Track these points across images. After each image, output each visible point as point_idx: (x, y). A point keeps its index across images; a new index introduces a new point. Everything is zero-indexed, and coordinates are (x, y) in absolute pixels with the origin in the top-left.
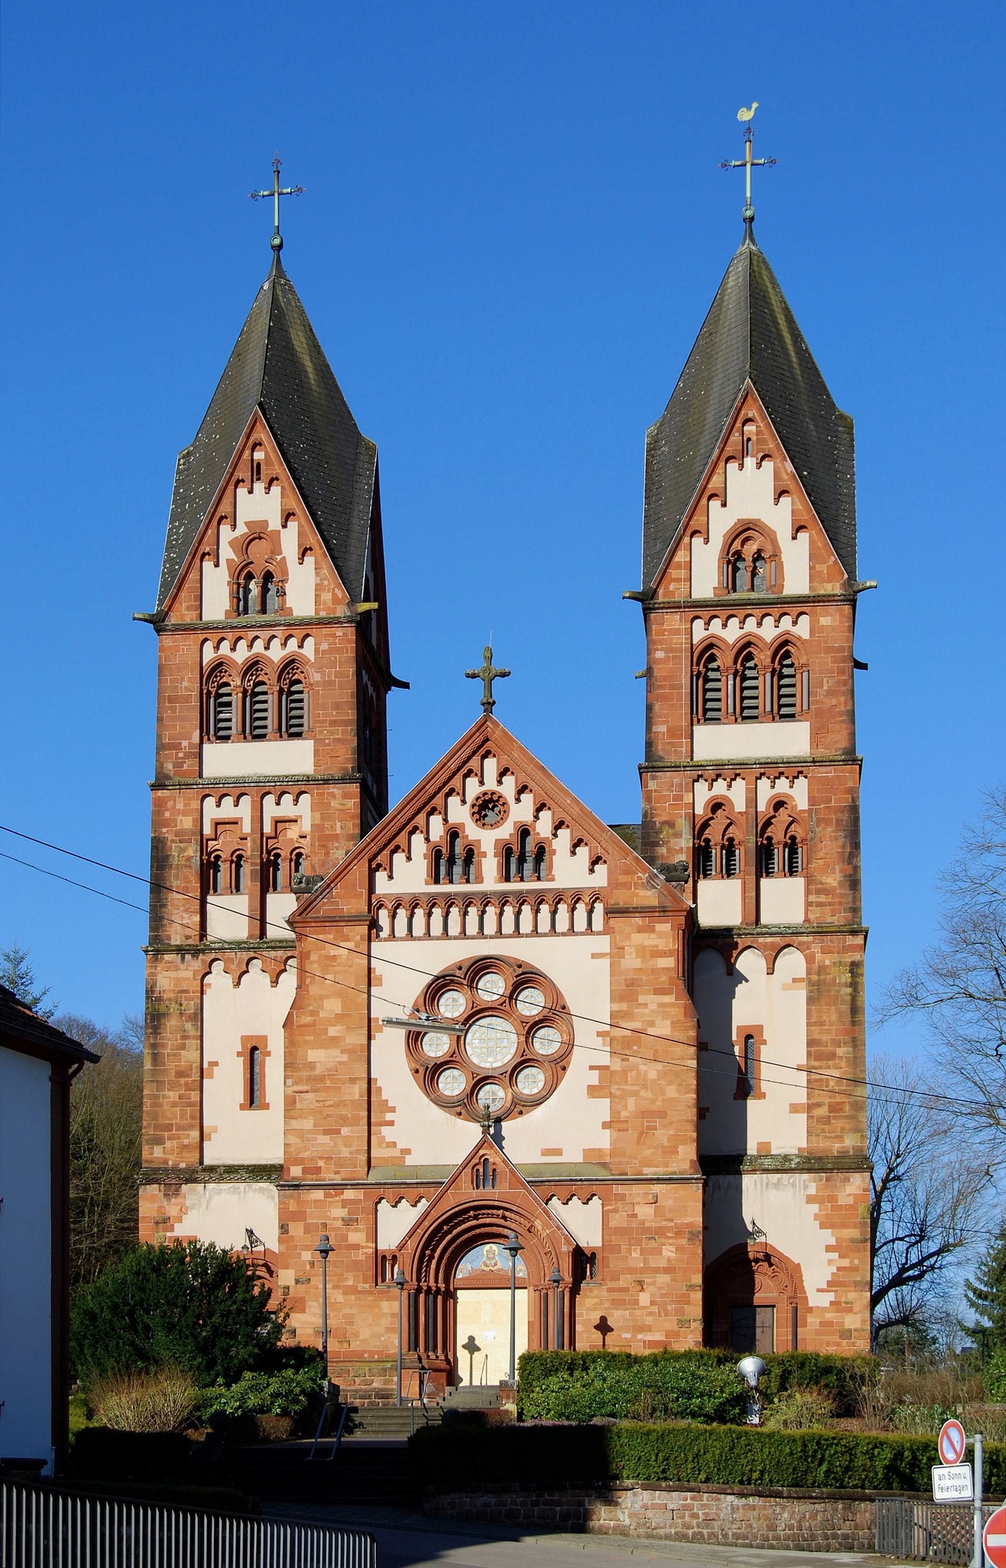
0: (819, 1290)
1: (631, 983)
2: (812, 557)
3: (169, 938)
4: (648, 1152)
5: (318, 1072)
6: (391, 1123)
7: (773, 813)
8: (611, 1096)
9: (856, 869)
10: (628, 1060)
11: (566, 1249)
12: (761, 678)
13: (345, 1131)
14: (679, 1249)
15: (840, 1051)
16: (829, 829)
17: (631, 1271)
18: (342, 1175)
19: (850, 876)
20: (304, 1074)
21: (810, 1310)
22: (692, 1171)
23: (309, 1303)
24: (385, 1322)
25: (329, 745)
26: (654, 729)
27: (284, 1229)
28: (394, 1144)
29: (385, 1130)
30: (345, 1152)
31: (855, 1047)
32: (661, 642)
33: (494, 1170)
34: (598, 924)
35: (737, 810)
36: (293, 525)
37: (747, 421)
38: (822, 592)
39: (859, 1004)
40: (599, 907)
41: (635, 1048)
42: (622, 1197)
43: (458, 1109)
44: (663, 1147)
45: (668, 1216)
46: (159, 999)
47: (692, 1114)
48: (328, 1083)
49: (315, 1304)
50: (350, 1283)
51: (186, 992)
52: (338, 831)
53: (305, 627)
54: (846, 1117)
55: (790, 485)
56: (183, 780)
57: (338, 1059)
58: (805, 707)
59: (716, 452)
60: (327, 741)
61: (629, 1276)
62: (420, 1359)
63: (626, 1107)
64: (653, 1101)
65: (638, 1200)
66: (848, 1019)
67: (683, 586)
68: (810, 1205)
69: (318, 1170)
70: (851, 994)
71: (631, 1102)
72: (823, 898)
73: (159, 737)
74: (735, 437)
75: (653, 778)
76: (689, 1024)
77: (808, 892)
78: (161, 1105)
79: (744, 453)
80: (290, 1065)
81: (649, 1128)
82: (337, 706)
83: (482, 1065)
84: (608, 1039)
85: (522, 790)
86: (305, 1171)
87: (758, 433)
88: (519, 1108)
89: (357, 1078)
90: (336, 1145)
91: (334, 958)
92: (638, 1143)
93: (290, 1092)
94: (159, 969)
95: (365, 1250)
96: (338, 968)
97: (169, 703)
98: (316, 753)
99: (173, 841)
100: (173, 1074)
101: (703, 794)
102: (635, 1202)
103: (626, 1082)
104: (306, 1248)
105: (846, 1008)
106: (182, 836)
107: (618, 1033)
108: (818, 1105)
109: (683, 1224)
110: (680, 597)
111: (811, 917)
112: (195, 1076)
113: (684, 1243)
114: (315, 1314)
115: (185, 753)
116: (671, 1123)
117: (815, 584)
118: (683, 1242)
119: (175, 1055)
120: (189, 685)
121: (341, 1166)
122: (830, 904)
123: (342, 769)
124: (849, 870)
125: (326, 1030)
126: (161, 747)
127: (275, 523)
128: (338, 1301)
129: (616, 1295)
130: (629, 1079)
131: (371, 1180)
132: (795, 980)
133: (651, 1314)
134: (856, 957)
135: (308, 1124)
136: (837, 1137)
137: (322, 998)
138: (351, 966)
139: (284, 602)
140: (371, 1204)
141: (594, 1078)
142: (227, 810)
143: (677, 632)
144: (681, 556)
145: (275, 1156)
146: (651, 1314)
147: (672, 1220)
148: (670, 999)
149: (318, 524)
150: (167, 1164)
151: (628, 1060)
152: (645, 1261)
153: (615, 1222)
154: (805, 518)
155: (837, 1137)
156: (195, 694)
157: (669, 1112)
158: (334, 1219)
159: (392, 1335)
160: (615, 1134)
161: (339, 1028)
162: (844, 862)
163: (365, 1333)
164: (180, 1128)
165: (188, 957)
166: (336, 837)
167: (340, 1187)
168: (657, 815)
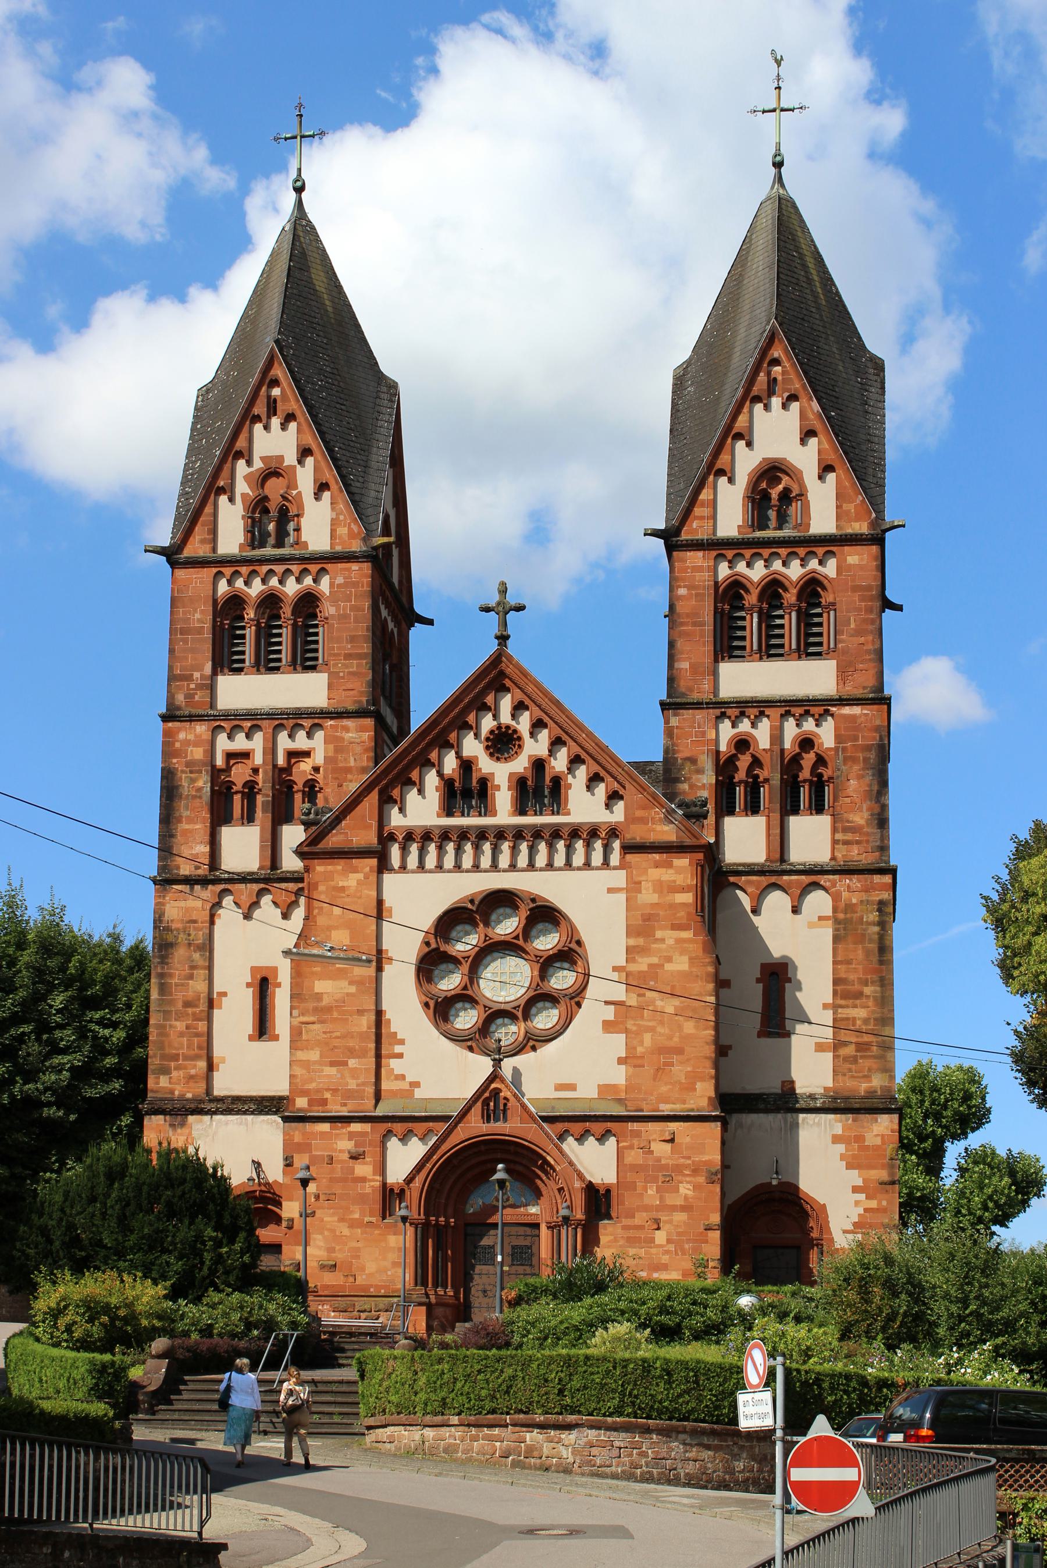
2: (839, 496)
4: (664, 1089)
6: (400, 1056)
8: (626, 1031)
9: (884, 808)
10: (644, 995)
11: (578, 1184)
12: (787, 617)
13: (352, 1063)
14: (696, 1187)
15: (868, 990)
16: (856, 768)
17: (646, 1208)
18: (350, 1107)
19: (879, 814)
20: (311, 1005)
22: (711, 1108)
25: (343, 678)
26: (676, 665)
27: (288, 1163)
28: (403, 1077)
29: (394, 1063)
30: (352, 1084)
32: (683, 579)
33: (505, 1105)
34: (615, 859)
35: (761, 747)
36: (310, 461)
37: (776, 362)
38: (850, 531)
39: (888, 943)
40: (616, 845)
42: (637, 1134)
44: (681, 1083)
45: (685, 1153)
47: (709, 1051)
48: (335, 1015)
49: (320, 1237)
50: (357, 1216)
52: (352, 763)
55: (818, 426)
56: (194, 711)
57: (346, 991)
58: (832, 645)
60: (341, 674)
61: (644, 1214)
62: (427, 1295)
63: (642, 1043)
64: (670, 1038)
65: (654, 1136)
66: (875, 958)
67: (708, 525)
69: (324, 1102)
71: (647, 1038)
72: (849, 837)
73: (171, 668)
74: (762, 377)
75: (675, 715)
76: (707, 960)
77: (834, 830)
79: (771, 393)
80: (296, 996)
81: (666, 1064)
82: (353, 639)
83: (495, 999)
85: (538, 725)
86: (311, 1102)
87: (784, 373)
88: (531, 1043)
92: (654, 1080)
93: (296, 1022)
95: (372, 1184)
97: (181, 634)
98: (330, 686)
99: (183, 772)
101: (726, 732)
103: (642, 1017)
105: (874, 946)
107: (633, 968)
108: (845, 1044)
110: (702, 535)
111: (838, 855)
112: (203, 1006)
114: (319, 1248)
115: (197, 685)
116: (688, 1060)
117: (843, 523)
118: (701, 1179)
120: (201, 617)
121: (348, 1098)
122: (858, 842)
123: (355, 702)
124: (877, 810)
126: (172, 678)
129: (631, 1233)
131: (379, 1112)
132: (820, 918)
133: (667, 1252)
135: (314, 1055)
137: (330, 928)
139: (299, 537)
140: (378, 1137)
141: (609, 1013)
143: (700, 569)
144: (705, 495)
145: (279, 1087)
146: (667, 1252)
147: (689, 1158)
149: (334, 460)
151: (644, 995)
152: (661, 1199)
153: (630, 1159)
154: (831, 458)
156: (208, 625)
157: (686, 1048)
158: (341, 1151)
160: (631, 1070)
162: (871, 800)
163: (371, 1267)
166: (348, 770)
168: (678, 751)
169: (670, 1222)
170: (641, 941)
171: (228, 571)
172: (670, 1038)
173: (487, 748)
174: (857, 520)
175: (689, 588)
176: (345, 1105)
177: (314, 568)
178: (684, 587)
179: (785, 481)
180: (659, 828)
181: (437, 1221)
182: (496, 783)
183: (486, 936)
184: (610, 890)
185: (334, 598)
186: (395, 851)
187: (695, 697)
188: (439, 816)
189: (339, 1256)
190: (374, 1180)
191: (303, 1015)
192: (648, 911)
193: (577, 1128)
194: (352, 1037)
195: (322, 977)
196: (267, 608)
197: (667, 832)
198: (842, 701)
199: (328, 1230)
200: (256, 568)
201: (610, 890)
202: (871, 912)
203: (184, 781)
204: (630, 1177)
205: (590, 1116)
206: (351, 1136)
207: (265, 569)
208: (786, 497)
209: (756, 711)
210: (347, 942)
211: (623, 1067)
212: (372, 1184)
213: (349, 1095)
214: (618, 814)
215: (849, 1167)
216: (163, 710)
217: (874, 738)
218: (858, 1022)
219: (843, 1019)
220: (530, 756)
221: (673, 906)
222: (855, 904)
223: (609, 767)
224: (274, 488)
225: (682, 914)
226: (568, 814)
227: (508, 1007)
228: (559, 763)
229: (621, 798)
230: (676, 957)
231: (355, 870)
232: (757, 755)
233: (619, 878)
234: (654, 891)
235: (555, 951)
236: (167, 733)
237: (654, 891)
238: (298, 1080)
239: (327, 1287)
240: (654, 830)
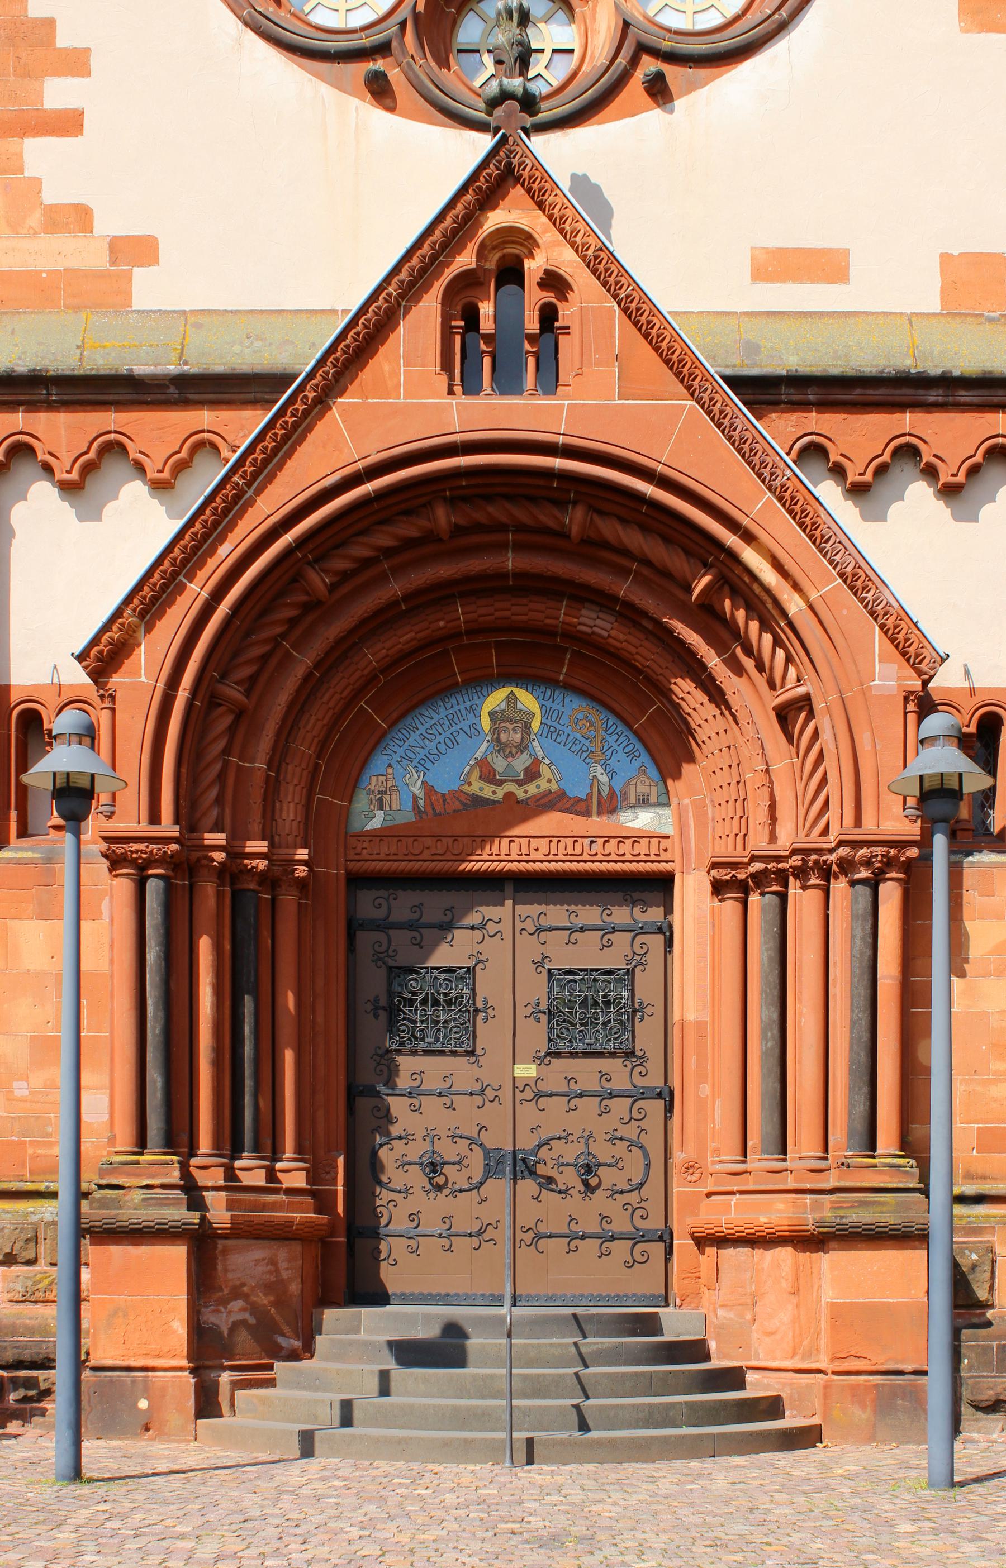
33: (548, 316)
88: (649, 65)
181: (235, 853)
205: (922, 382)
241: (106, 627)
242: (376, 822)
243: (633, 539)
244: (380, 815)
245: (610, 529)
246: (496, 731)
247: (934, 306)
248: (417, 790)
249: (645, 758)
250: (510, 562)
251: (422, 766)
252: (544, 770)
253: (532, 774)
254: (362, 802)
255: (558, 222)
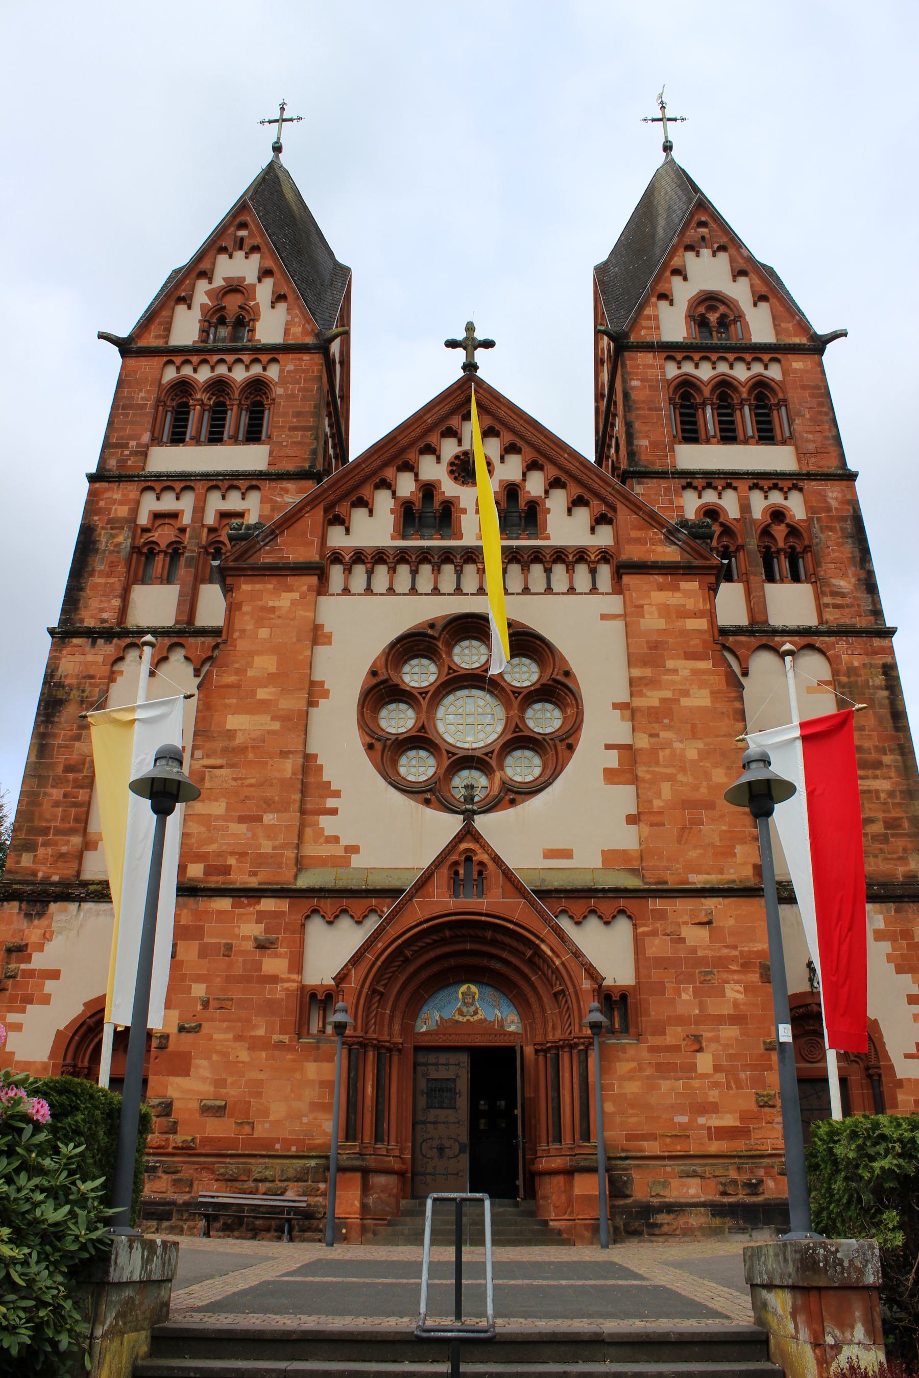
0: (908, 1056)
1: (655, 646)
3: (82, 621)
4: (693, 854)
5: (240, 740)
6: (334, 812)
7: (770, 521)
9: (870, 574)
10: (657, 735)
13: (268, 818)
15: (887, 759)
17: (681, 1020)
19: (866, 580)
20: (219, 745)
21: (900, 1083)
23: (196, 1062)
24: (311, 1094)
25: (286, 446)
26: (635, 442)
28: (336, 840)
29: (325, 821)
30: (267, 847)
31: (903, 754)
32: (636, 374)
33: (480, 873)
39: (900, 708)
41: (666, 721)
42: (661, 915)
43: (428, 796)
45: (729, 941)
46: (60, 685)
48: (251, 756)
49: (204, 1063)
50: (261, 1032)
51: (92, 677)
53: (274, 352)
54: (908, 835)
57: (267, 728)
58: (787, 434)
59: (675, 240)
60: (285, 444)
61: (679, 1029)
63: (659, 795)
65: (686, 918)
66: (889, 724)
68: (879, 943)
69: (226, 870)
70: (888, 698)
71: (666, 789)
73: (107, 438)
75: (639, 483)
76: (733, 695)
77: (817, 597)
78: (39, 805)
82: (298, 415)
84: (627, 713)
89: (290, 752)
90: (255, 837)
91: (273, 609)
92: (679, 841)
94: (64, 652)
95: (286, 985)
96: (278, 621)
97: (123, 409)
99: (103, 528)
100: (59, 770)
102: (680, 921)
103: (657, 763)
104: (199, 979)
105: (885, 712)
106: (115, 524)
107: (638, 702)
109: (750, 952)
113: (755, 980)
114: (204, 1079)
116: (722, 816)
118: (755, 977)
119: (66, 747)
123: (297, 467)
124: (863, 575)
125: (253, 693)
127: (251, 277)
128: (241, 1059)
129: (663, 1058)
130: (661, 759)
131: (303, 882)
133: (716, 1085)
134: (889, 660)
136: (900, 858)
137: (252, 654)
138: (294, 619)
142: (168, 503)
143: (652, 367)
144: (648, 311)
146: (716, 1085)
147: (735, 947)
148: (706, 665)
150: (35, 875)
151: (657, 735)
152: (702, 1006)
155: (900, 858)
158: (245, 938)
159: (321, 1115)
160: (646, 830)
161: (271, 689)
163: (278, 1110)
164: (58, 832)
165: (100, 642)
167: (255, 894)
169: (716, 1039)
170: (647, 672)
171: (178, 360)
172: (696, 788)
173: (451, 472)
174: (796, 336)
175: (642, 380)
176: (255, 874)
177: (264, 358)
178: (637, 379)
179: (722, 309)
180: (659, 549)
182: (462, 506)
183: (450, 668)
184: (604, 617)
185: (283, 380)
186: (336, 573)
187: (658, 468)
188: (393, 538)
189: (232, 1092)
190: (289, 980)
191: (207, 755)
192: (654, 638)
193: (578, 907)
194: (271, 785)
195: (237, 711)
196: (213, 394)
197: (669, 553)
198: (809, 476)
199: (217, 1052)
200: (207, 357)
201: (604, 617)
202: (876, 675)
203: (103, 539)
204: (656, 975)
206: (261, 917)
207: (216, 358)
208: (723, 323)
209: (723, 482)
210: (273, 669)
211: (634, 828)
212: (286, 985)
213: (261, 860)
214: (604, 537)
215: (899, 970)
216: (93, 470)
217: (848, 511)
218: (883, 796)
219: (865, 792)
220: (501, 481)
221: (684, 633)
222: (856, 667)
223: (596, 486)
224: (232, 303)
225: (696, 641)
226: (548, 538)
227: (477, 754)
228: (535, 485)
229: (609, 522)
230: (694, 691)
231: (290, 589)
232: (728, 523)
233: (614, 604)
234: (660, 616)
235: (538, 686)
236: (92, 495)
237: (660, 616)
238: (193, 840)
239: (207, 1141)
240: (653, 551)
241: (342, 969)
242: (424, 1029)
243: (507, 940)
244: (425, 1027)
245: (499, 937)
246: (464, 998)
247: (601, 866)
248: (437, 1018)
249: (512, 1008)
250: (468, 946)
251: (439, 1010)
252: (480, 1012)
253: (476, 1013)
254: (419, 1022)
255: (483, 847)
